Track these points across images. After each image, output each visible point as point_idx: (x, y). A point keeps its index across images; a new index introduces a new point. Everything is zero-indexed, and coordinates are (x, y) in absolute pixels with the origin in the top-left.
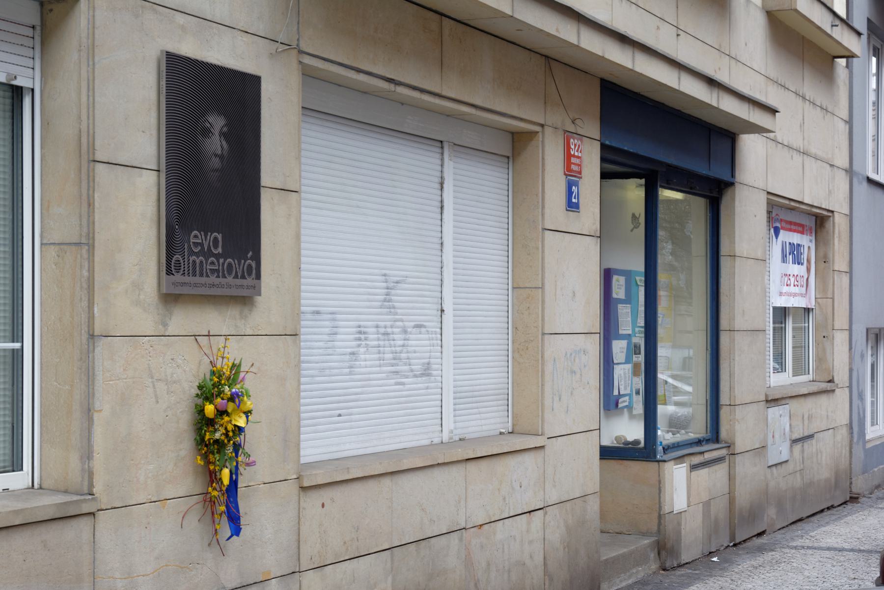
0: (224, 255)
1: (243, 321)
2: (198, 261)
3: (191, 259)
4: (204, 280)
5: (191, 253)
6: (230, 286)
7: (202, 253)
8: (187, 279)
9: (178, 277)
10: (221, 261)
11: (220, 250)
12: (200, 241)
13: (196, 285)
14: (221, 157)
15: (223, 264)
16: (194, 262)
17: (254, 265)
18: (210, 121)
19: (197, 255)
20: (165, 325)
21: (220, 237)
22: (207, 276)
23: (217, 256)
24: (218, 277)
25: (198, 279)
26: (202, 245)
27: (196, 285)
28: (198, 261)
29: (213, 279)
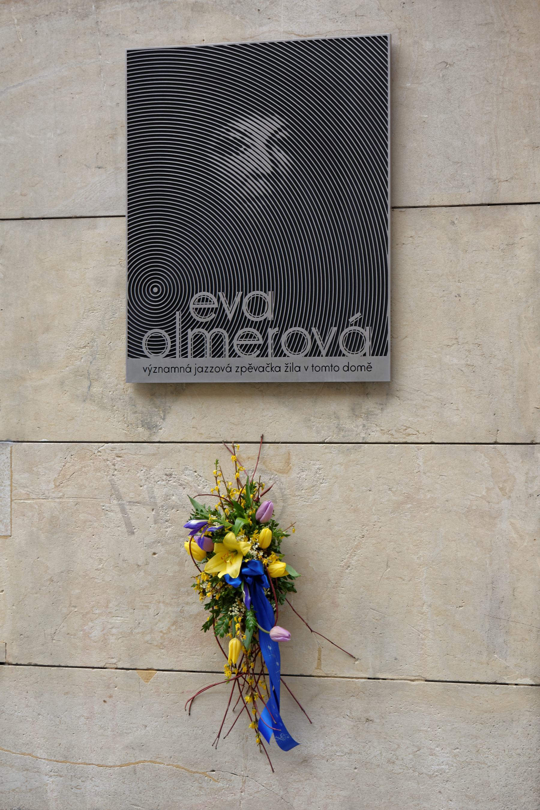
0: (282, 321)
1: (360, 421)
2: (208, 336)
3: (191, 334)
4: (234, 362)
5: (189, 323)
8: (179, 361)
9: (158, 360)
10: (271, 332)
11: (269, 315)
12: (216, 305)
13: (202, 370)
14: (274, 177)
15: (277, 338)
17: (366, 333)
18: (242, 128)
19: (208, 326)
20: (151, 427)
21: (269, 297)
22: (233, 354)
23: (262, 327)
24: (264, 354)
25: (208, 360)
26: (220, 310)
27: (202, 370)
28: (208, 336)
29: (252, 359)
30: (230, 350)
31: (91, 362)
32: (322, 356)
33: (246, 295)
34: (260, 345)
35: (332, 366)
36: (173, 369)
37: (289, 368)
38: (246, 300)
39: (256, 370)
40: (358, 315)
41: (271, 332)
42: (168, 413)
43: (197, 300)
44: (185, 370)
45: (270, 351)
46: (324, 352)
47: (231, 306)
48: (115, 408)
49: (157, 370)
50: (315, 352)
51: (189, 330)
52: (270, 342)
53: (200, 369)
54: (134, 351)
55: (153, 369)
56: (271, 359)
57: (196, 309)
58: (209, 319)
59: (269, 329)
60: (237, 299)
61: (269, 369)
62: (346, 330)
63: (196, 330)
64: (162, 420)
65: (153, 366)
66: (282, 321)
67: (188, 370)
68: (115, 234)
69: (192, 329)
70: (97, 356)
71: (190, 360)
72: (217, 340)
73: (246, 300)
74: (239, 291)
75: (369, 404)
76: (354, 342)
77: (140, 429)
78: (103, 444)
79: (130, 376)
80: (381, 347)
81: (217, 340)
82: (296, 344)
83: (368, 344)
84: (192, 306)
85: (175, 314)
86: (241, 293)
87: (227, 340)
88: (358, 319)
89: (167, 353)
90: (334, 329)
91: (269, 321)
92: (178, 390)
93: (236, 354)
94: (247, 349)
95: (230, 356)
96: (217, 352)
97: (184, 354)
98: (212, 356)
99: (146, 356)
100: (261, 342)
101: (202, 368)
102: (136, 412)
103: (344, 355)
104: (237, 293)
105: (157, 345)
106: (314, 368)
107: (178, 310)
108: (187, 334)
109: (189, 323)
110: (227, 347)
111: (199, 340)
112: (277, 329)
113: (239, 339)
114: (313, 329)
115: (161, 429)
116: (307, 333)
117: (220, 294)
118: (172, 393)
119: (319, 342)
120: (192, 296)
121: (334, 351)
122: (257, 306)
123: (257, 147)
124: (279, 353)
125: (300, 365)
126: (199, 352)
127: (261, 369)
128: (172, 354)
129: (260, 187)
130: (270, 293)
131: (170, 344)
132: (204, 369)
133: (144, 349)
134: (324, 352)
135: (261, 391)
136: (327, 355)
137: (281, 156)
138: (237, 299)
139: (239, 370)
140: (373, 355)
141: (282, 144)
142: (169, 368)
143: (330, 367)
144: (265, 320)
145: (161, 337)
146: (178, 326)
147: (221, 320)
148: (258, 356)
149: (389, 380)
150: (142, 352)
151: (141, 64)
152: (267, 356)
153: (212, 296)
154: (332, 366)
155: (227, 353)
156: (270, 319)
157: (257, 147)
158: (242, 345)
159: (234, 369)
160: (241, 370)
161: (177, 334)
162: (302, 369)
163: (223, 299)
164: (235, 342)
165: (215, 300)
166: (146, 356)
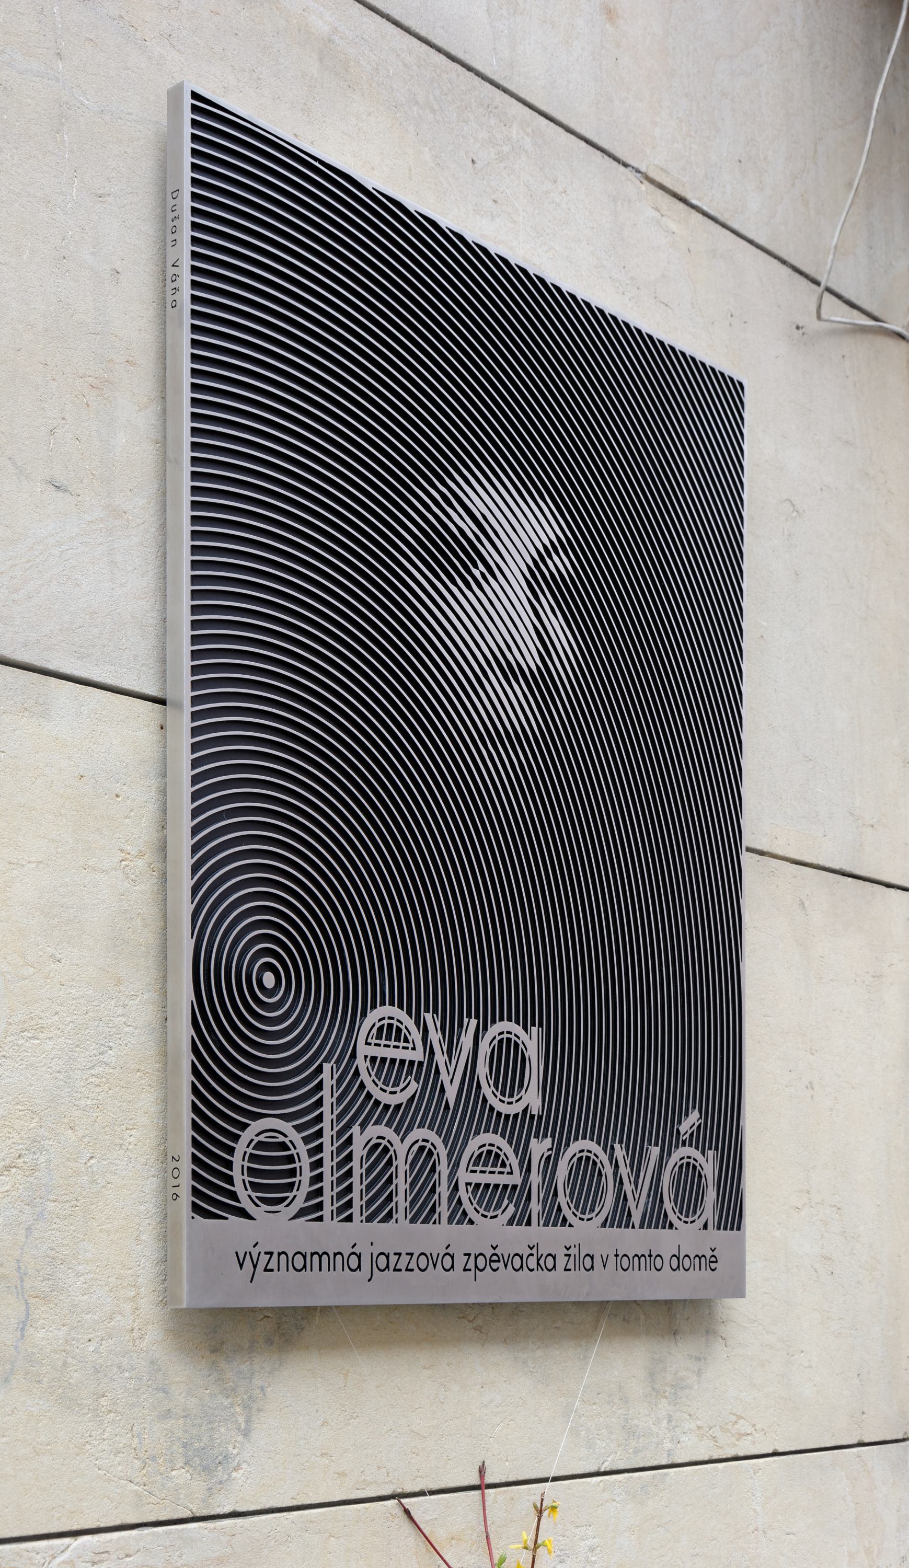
0: (557, 1122)
1: (664, 1406)
2: (401, 1149)
3: (360, 1140)
6: (584, 1261)
7: (428, 1107)
8: (331, 1234)
9: (275, 1228)
10: (539, 1148)
11: (532, 1098)
12: (418, 1055)
13: (387, 1262)
14: (540, 683)
16: (380, 1153)
17: (708, 1166)
18: (478, 507)
20: (210, 1463)
21: (531, 1042)
22: (459, 1216)
24: (522, 1219)
25: (400, 1234)
26: (426, 1071)
27: (387, 1262)
29: (493, 1231)
30: (450, 1199)
31: (29, 1229)
32: (633, 1227)
33: (485, 1029)
34: (515, 1187)
35: (650, 1256)
36: (316, 1257)
37: (572, 1257)
38: (485, 1048)
39: (506, 1266)
41: (539, 1148)
42: (259, 1410)
43: (374, 1031)
44: (345, 1264)
46: (636, 1218)
47: (454, 1062)
48: (103, 1401)
49: (273, 1265)
51: (356, 1129)
52: (535, 1179)
53: (382, 1261)
55: (264, 1258)
57: (373, 1059)
58: (402, 1098)
59: (533, 1141)
60: (467, 1041)
61: (532, 1262)
63: (373, 1131)
64: (240, 1438)
65: (262, 1248)
67: (354, 1262)
69: (363, 1126)
70: (51, 1206)
73: (485, 1048)
74: (469, 1016)
75: (678, 1356)
77: (181, 1475)
78: (67, 1541)
84: (362, 1050)
85: (320, 1070)
86: (474, 1022)
88: (695, 1128)
89: (299, 1203)
90: (655, 1151)
91: (532, 1117)
92: (286, 1330)
93: (465, 1213)
94: (489, 1196)
95: (450, 1221)
98: (409, 1217)
99: (243, 1213)
100: (516, 1179)
101: (388, 1257)
102: (167, 1415)
103: (471, 1222)
104: (466, 1020)
105: (273, 1176)
106: (653, 1259)
107: (327, 1060)
108: (349, 1141)
112: (548, 1142)
113: (471, 1168)
114: (617, 1146)
115: (236, 1469)
117: (428, 1017)
118: (269, 1342)
120: (364, 1015)
127: (517, 1262)
128: (313, 1210)
129: (510, 704)
130: (534, 1030)
131: (307, 1174)
132: (393, 1259)
133: (238, 1188)
134: (636, 1218)
135: (478, 1329)
136: (642, 1226)
138: (467, 1041)
139: (471, 1265)
140: (546, 1224)
142: (305, 1257)
143: (648, 1258)
144: (525, 1110)
145: (283, 1146)
148: (510, 1222)
150: (234, 1196)
152: (529, 1223)
153: (409, 1023)
154: (650, 1256)
155: (444, 1210)
156: (535, 1112)
158: (478, 1186)
159: (460, 1261)
161: (326, 1139)
162: (598, 1261)
163: (435, 1036)
165: (416, 1036)
166: (243, 1213)
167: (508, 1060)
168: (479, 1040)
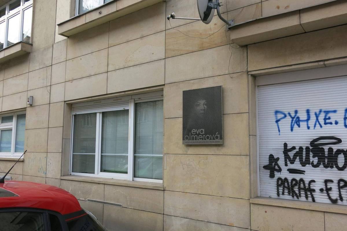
0: (206, 134)
2: (194, 136)
3: (192, 136)
5: (192, 134)
7: (196, 134)
8: (190, 141)
11: (204, 133)
13: (193, 142)
14: (204, 110)
17: (219, 136)
18: (199, 102)
19: (194, 135)
21: (203, 130)
22: (198, 140)
23: (203, 135)
24: (203, 140)
25: (194, 141)
26: (196, 132)
29: (201, 140)
40: (217, 133)
41: (204, 136)
45: (204, 139)
50: (211, 139)
54: (183, 139)
56: (204, 140)
58: (194, 134)
60: (199, 130)
62: (216, 135)
66: (206, 134)
68: (181, 120)
71: (192, 141)
72: (196, 137)
75: (220, 148)
76: (217, 138)
79: (183, 143)
80: (221, 138)
81: (196, 137)
82: (208, 138)
83: (219, 138)
87: (197, 137)
94: (200, 139)
96: (196, 139)
97: (191, 140)
105: (187, 138)
109: (192, 134)
110: (197, 138)
111: (193, 137)
116: (209, 136)
119: (211, 138)
121: (214, 139)
122: (202, 131)
123: (201, 105)
124: (205, 139)
125: (208, 141)
126: (193, 139)
128: (189, 140)
129: (202, 112)
137: (205, 106)
138: (199, 130)
141: (205, 104)
146: (190, 135)
147: (196, 134)
149: (222, 144)
151: (185, 93)
157: (201, 105)
160: (199, 142)
164: (199, 137)
167: (202, 131)
168: (200, 130)
